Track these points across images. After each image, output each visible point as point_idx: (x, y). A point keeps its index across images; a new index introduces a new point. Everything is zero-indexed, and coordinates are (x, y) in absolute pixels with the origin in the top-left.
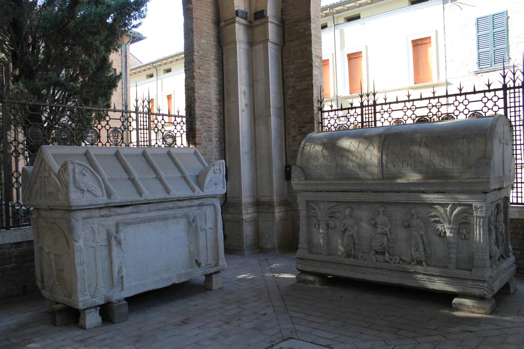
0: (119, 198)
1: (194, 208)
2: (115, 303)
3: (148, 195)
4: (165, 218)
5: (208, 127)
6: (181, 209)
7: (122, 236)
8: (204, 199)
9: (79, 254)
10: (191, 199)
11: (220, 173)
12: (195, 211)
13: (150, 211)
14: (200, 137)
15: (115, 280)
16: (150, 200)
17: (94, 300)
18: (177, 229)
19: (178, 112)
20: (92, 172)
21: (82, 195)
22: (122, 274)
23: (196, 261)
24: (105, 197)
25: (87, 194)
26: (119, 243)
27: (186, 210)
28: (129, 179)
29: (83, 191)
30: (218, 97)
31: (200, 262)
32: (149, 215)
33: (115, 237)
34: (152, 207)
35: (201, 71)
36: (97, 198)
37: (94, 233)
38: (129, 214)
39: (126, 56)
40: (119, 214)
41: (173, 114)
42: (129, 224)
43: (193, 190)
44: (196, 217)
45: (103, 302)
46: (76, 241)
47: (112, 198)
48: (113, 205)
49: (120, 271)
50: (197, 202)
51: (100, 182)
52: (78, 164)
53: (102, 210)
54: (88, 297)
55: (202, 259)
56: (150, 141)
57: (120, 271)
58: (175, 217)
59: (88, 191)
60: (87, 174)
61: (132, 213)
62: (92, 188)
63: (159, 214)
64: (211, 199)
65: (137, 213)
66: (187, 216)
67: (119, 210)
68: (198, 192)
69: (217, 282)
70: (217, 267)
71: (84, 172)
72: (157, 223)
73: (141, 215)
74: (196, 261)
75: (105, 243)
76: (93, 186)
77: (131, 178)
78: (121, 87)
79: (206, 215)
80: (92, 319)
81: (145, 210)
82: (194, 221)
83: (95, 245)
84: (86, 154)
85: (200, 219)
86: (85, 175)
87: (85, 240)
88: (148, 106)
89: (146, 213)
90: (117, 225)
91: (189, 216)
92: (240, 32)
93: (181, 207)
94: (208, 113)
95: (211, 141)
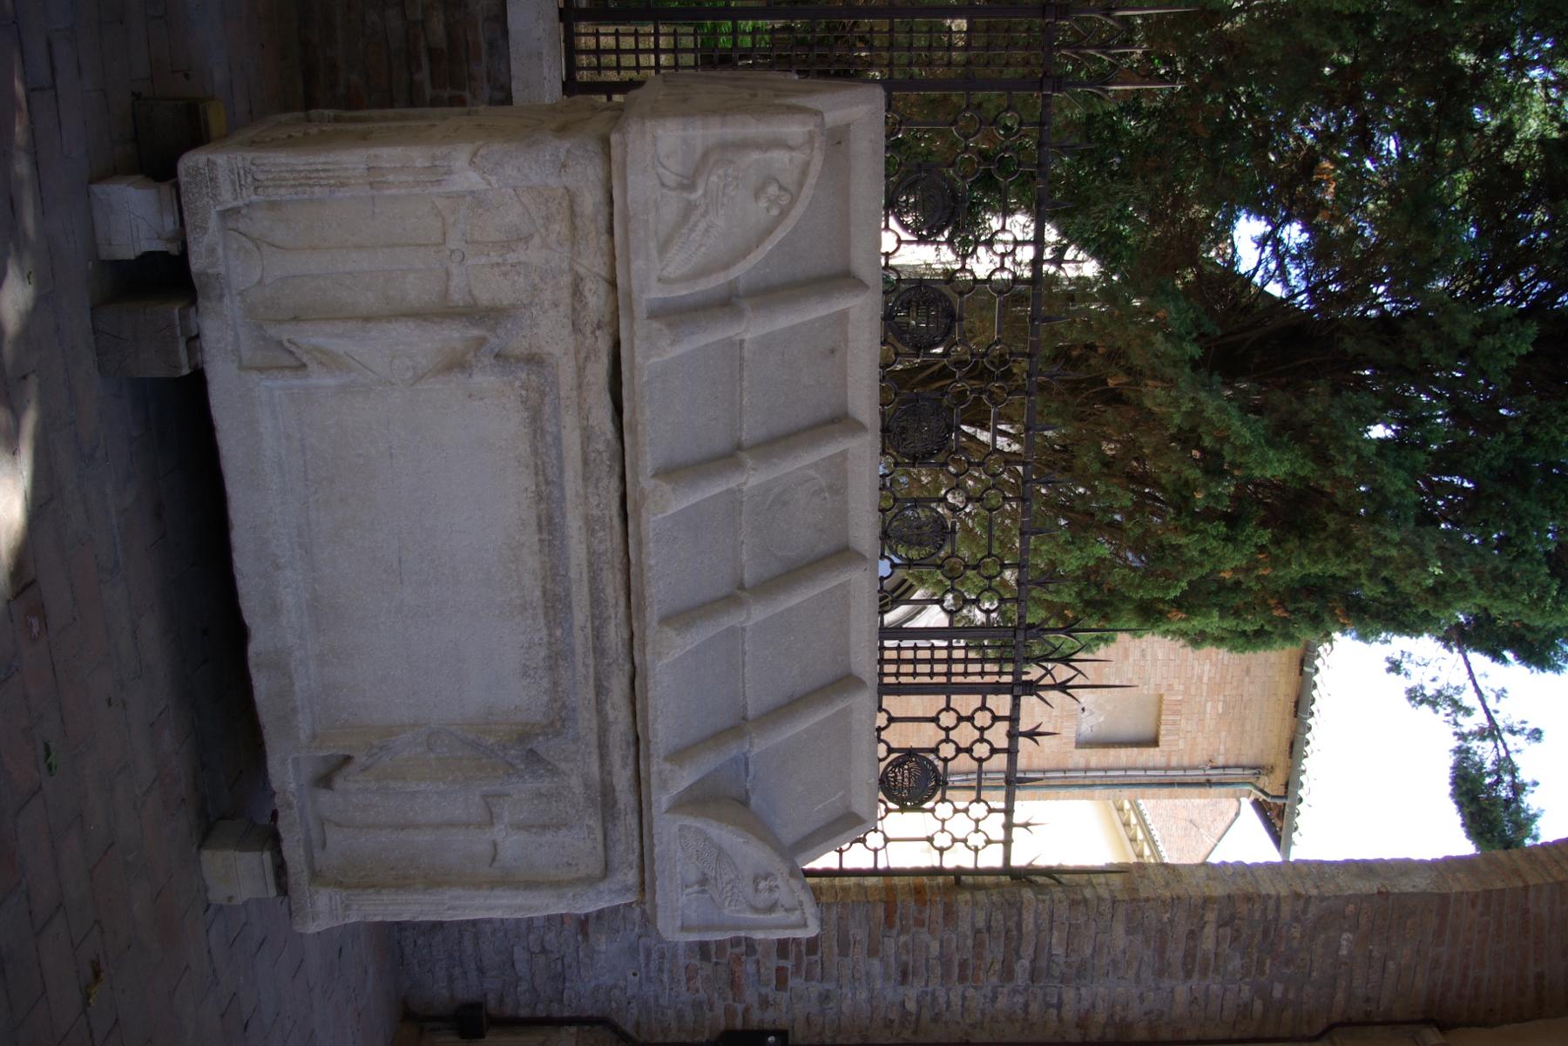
1: (595, 768)
2: (184, 317)
3: (664, 507)
4: (555, 604)
5: (963, 965)
6: (591, 694)
8: (632, 820)
9: (419, 163)
10: (637, 741)
11: (756, 910)
13: (591, 532)
14: (920, 923)
15: (286, 333)
16: (638, 526)
17: (213, 223)
19: (1026, 825)
20: (769, 232)
21: (671, 179)
22: (313, 366)
23: (348, 759)
24: (657, 293)
25: (671, 207)
26: (456, 365)
27: (586, 721)
28: (739, 447)
29: (688, 185)
31: (339, 783)
33: (481, 342)
34: (609, 541)
35: (1209, 930)
36: (654, 253)
37: (506, 246)
38: (581, 417)
39: (1209, 783)
40: (581, 370)
41: (1017, 805)
43: (679, 755)
44: (554, 772)
45: (197, 264)
46: (475, 154)
47: (655, 325)
48: (623, 336)
49: (331, 361)
50: (622, 779)
51: (726, 266)
52: (807, 164)
53: (603, 288)
54: (227, 198)
56: (900, 690)
57: (331, 361)
58: (558, 657)
59: (690, 208)
60: (763, 204)
61: (587, 436)
62: (702, 225)
63: (573, 574)
64: (634, 858)
65: (586, 462)
66: (559, 721)
67: (599, 371)
68: (672, 781)
69: (236, 874)
70: (305, 876)
71: (773, 190)
72: (532, 562)
74: (348, 759)
75: (457, 298)
76: (707, 230)
77: (744, 456)
78: (1093, 764)
79: (558, 827)
80: (133, 218)
81: (594, 501)
82: (533, 757)
83: (452, 245)
84: (843, 554)
85: (540, 795)
86: (757, 196)
87: (478, 200)
88: (1048, 680)
89: (584, 503)
90: (534, 360)
91: (558, 734)
93: (600, 690)
94: (1026, 963)
95: (904, 975)
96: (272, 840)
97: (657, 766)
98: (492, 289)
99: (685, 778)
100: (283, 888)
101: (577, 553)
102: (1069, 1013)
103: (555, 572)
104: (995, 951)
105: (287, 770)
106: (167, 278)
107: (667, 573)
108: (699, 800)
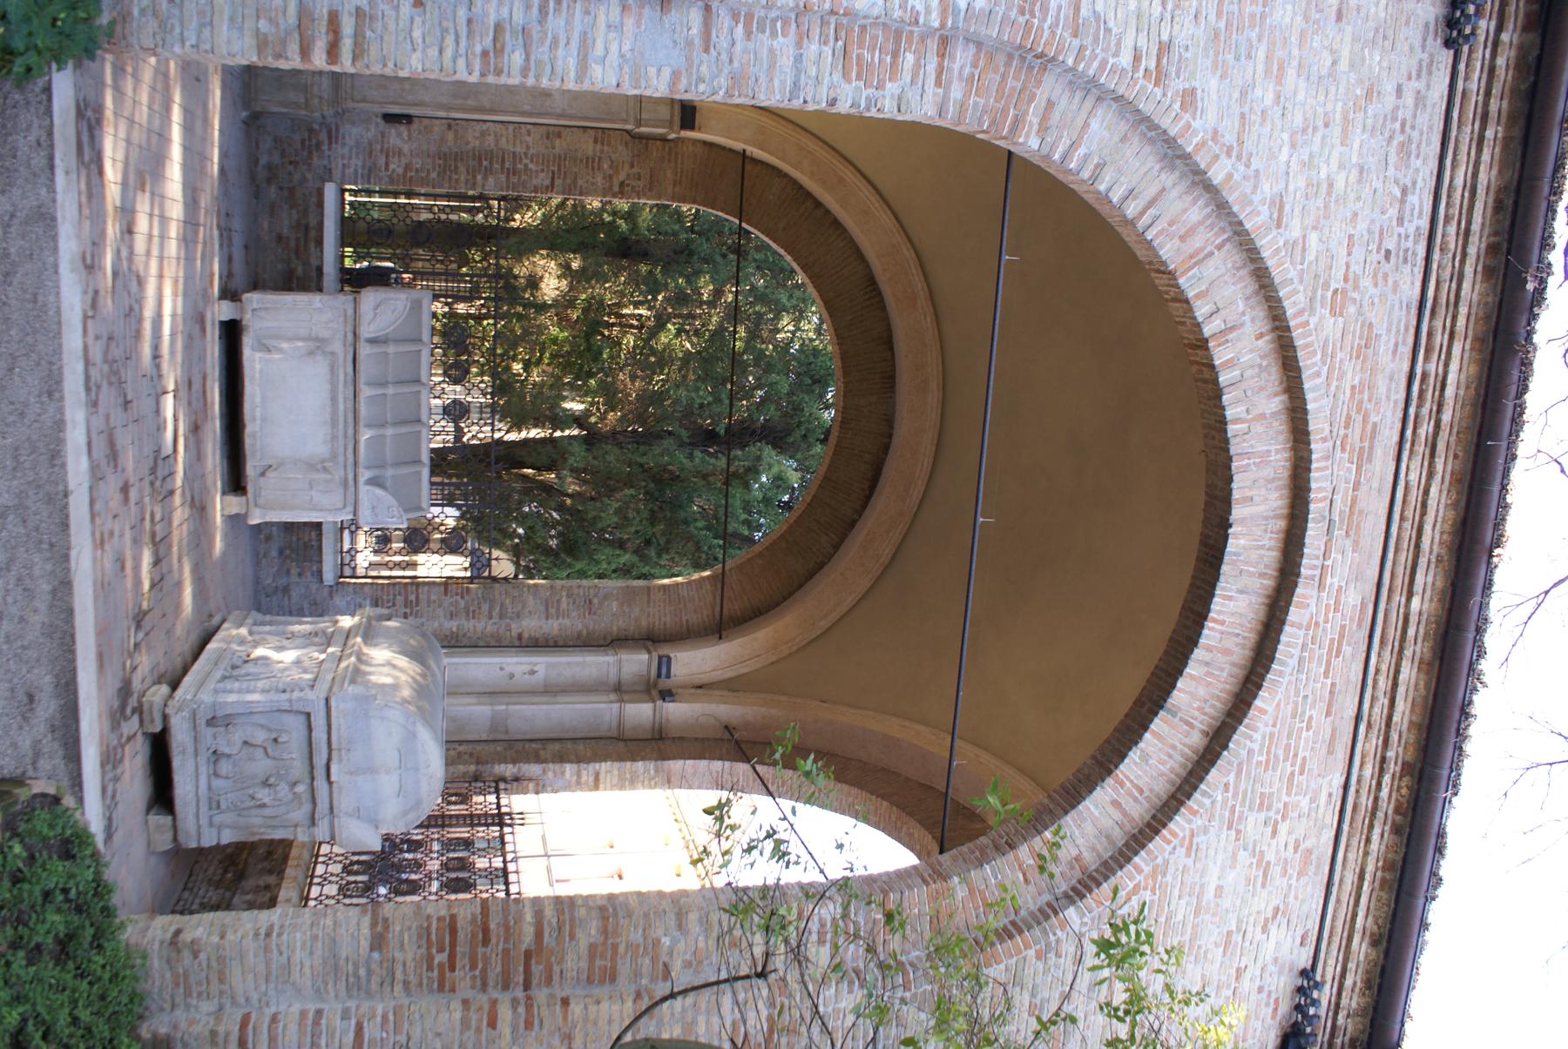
4: (334, 422)
7: (319, 358)
12: (338, 474)
24: (367, 335)
26: (311, 353)
27: (341, 459)
32: (341, 400)
34: (350, 404)
49: (280, 351)
50: (351, 476)
54: (255, 306)
57: (280, 351)
58: (334, 438)
68: (365, 475)
72: (329, 409)
89: (344, 393)
90: (332, 353)
92: (636, 662)
98: (324, 334)
101: (341, 407)
102: (514, 633)
104: (485, 607)
105: (251, 469)
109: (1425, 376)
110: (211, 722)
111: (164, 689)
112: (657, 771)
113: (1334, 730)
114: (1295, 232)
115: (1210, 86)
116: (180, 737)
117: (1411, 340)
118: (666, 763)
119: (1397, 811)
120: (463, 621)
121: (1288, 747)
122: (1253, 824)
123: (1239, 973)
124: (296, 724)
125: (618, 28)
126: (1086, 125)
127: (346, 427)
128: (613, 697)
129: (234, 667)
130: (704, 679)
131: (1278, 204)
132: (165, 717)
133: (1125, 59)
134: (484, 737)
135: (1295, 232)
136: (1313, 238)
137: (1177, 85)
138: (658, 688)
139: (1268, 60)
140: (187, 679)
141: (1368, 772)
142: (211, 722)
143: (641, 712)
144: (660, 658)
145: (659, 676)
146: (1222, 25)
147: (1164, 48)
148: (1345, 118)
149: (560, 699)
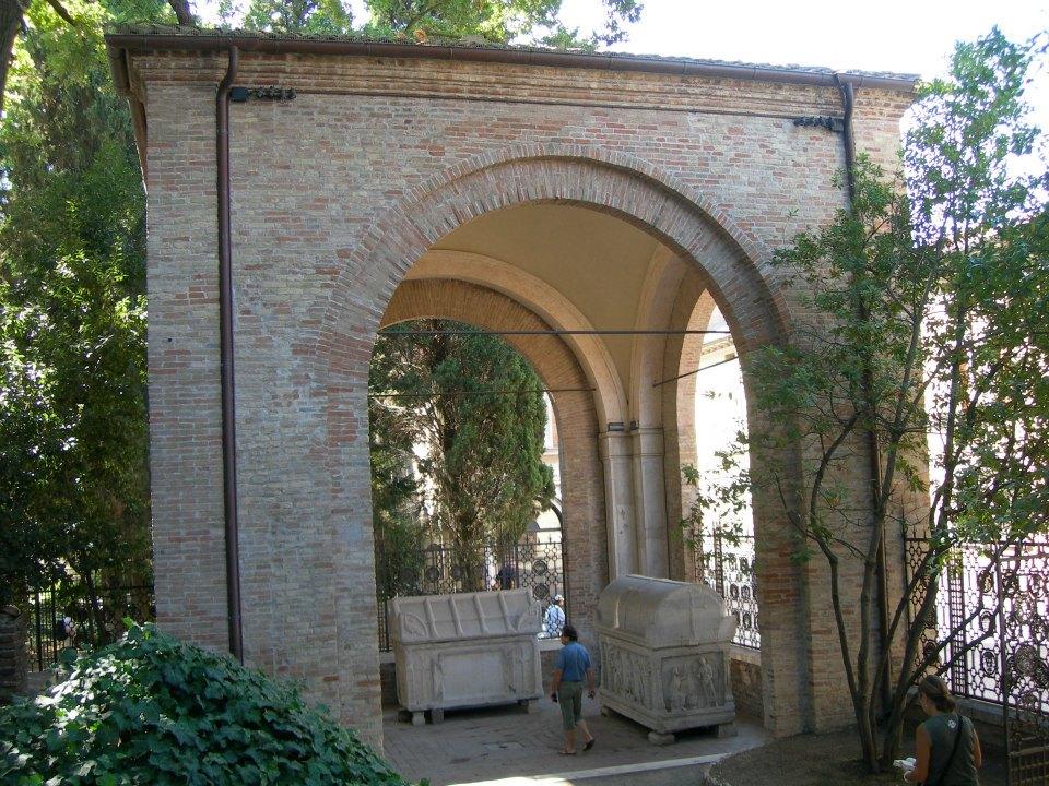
0: (439, 634)
3: (463, 632)
4: (481, 651)
10: (504, 636)
18: (492, 662)
24: (428, 636)
26: (440, 669)
30: (598, 517)
32: (467, 648)
34: (469, 643)
38: (449, 648)
42: (448, 655)
49: (440, 688)
55: (516, 686)
57: (440, 688)
58: (490, 651)
66: (501, 650)
67: (441, 645)
73: (458, 649)
80: (419, 719)
89: (462, 647)
90: (439, 655)
92: (613, 446)
96: (527, 700)
97: (509, 633)
98: (428, 661)
99: (511, 627)
100: (537, 699)
101: (472, 648)
102: (598, 524)
103: (475, 652)
104: (581, 544)
105: (513, 698)
106: (428, 715)
107: (473, 632)
108: (515, 625)
109: (470, 91)
110: (669, 709)
111: (651, 735)
112: (684, 434)
113: (664, 123)
114: (403, 183)
115: (335, 241)
116: (676, 725)
117: (451, 102)
118: (679, 428)
119: (708, 83)
120: (592, 558)
121: (674, 152)
122: (715, 168)
123: (796, 165)
124: (668, 666)
125: (348, 553)
126: (360, 307)
127: (484, 644)
128: (636, 460)
129: (636, 699)
130: (623, 399)
131: (389, 194)
132: (667, 733)
133: (328, 293)
134: (665, 542)
135: (403, 183)
136: (405, 171)
137: (336, 261)
138: (629, 430)
139: (317, 208)
140: (646, 724)
141: (687, 100)
142: (669, 709)
143: (645, 443)
144: (609, 430)
145: (622, 430)
146: (302, 238)
147: (319, 271)
148: (339, 157)
149: (639, 494)
